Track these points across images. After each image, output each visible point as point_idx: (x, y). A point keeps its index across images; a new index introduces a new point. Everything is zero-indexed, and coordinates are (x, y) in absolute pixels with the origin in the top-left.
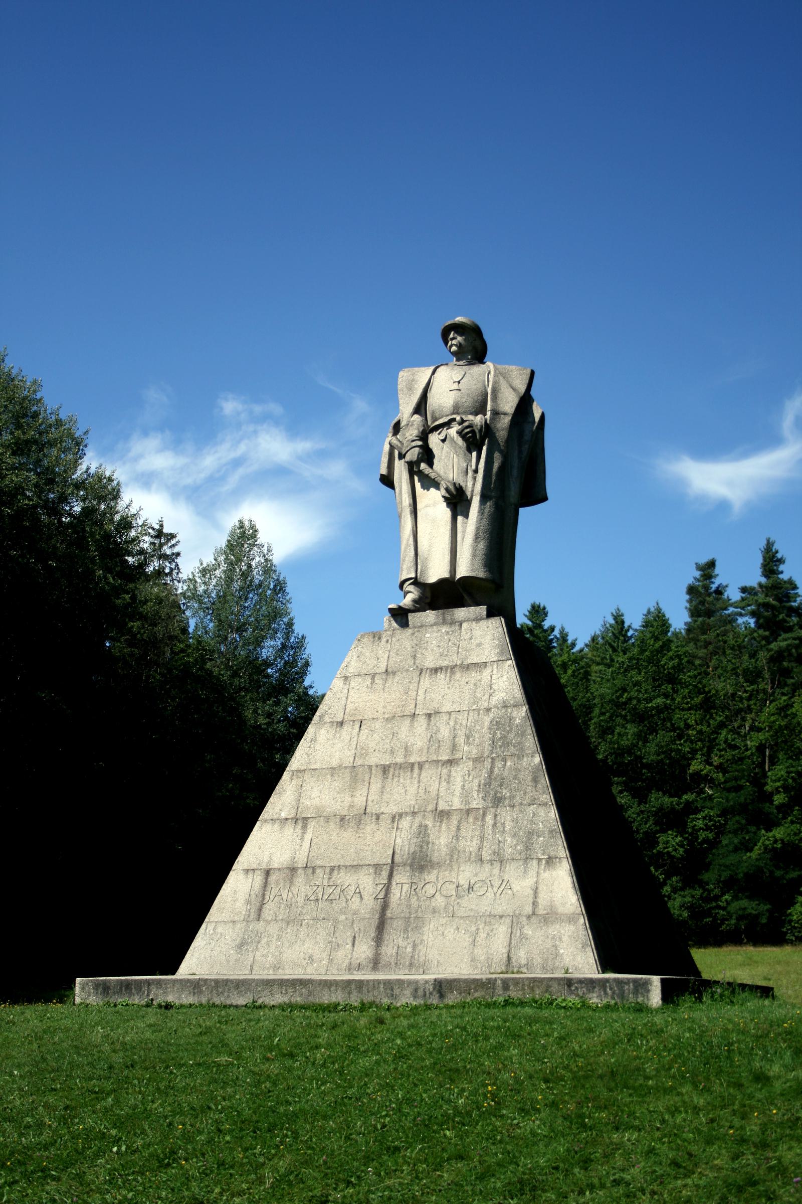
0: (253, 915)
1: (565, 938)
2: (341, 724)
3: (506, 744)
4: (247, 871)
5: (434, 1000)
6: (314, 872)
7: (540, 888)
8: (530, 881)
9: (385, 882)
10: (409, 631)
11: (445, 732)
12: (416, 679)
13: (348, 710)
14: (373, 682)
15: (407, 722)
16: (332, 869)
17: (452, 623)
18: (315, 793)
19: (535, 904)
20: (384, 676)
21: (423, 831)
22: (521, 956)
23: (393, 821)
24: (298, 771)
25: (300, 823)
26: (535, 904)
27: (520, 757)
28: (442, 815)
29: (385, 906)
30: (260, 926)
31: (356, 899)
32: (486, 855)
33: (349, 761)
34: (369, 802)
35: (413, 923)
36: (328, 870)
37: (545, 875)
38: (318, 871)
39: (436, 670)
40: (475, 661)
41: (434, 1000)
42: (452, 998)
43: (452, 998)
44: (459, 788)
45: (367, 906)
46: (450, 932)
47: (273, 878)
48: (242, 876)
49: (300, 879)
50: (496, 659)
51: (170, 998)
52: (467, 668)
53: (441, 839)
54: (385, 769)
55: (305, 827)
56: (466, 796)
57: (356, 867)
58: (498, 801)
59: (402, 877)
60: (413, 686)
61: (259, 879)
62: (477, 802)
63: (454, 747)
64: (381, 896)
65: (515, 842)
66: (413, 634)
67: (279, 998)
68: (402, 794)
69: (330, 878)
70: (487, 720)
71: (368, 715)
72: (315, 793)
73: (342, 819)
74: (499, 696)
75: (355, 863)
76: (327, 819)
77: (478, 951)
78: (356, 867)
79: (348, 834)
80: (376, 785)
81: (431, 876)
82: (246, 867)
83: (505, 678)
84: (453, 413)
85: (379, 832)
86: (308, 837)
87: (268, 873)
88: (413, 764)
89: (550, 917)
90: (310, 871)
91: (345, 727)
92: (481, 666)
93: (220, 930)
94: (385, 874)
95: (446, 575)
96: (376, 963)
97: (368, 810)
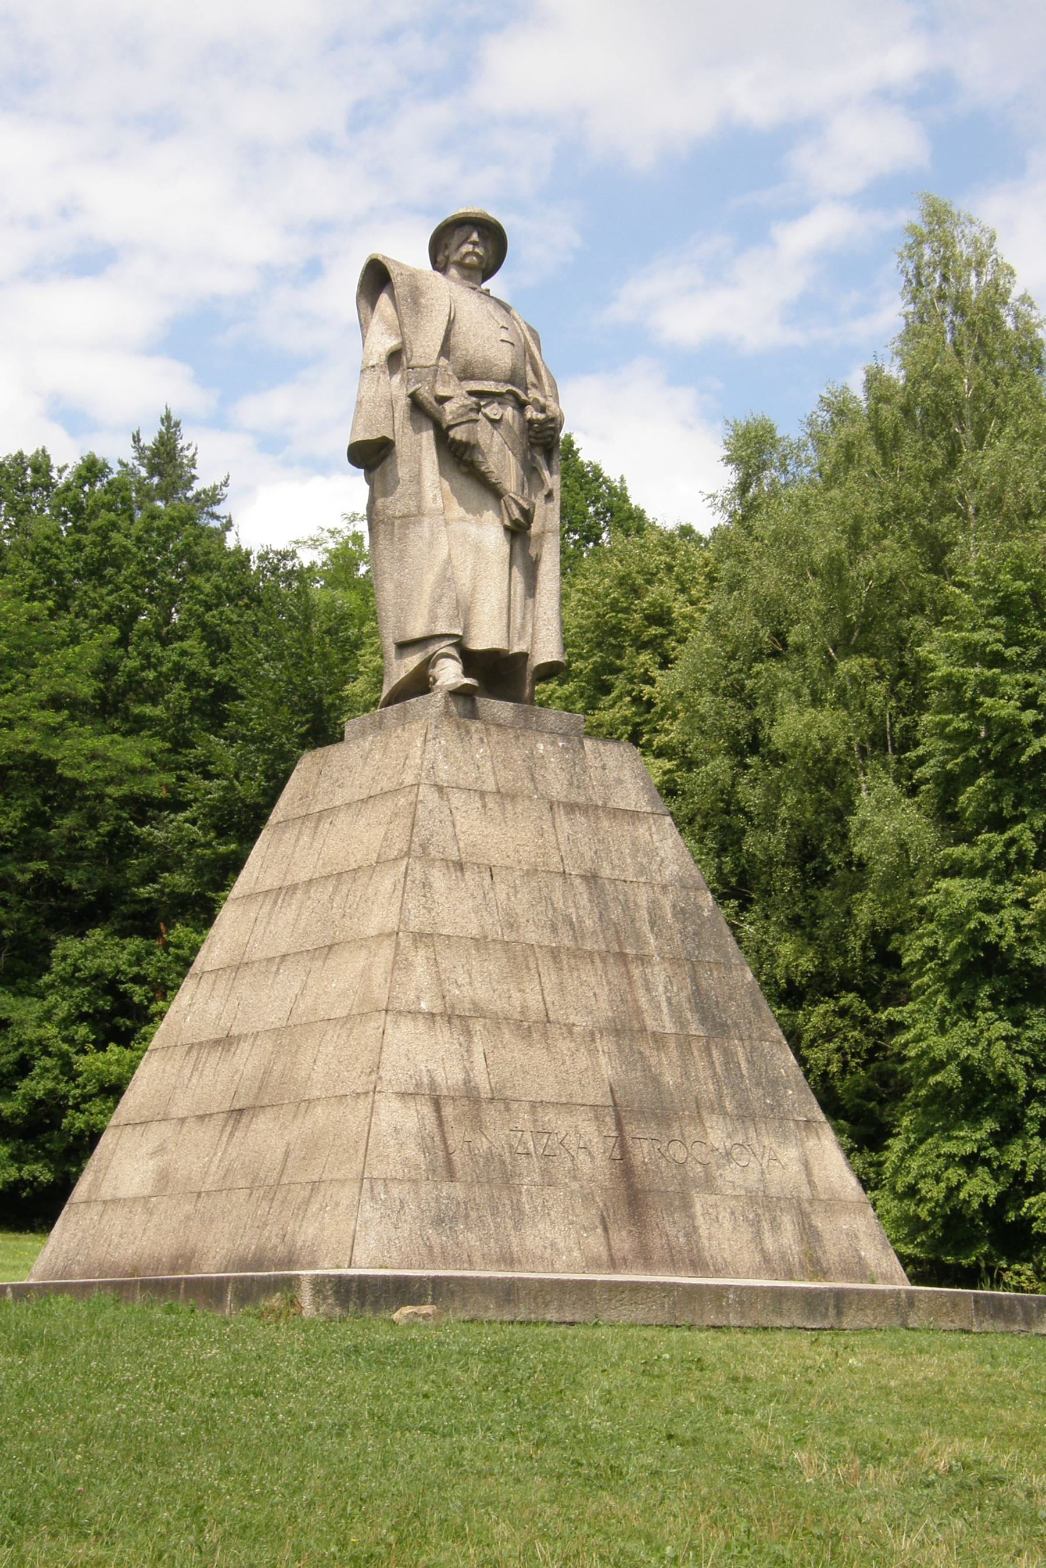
0: (441, 1171)
1: (861, 1236)
2: (460, 866)
4: (403, 1095)
6: (507, 1109)
7: (811, 1161)
9: (614, 1134)
10: (475, 726)
12: (547, 816)
13: (462, 844)
14: (484, 806)
15: (558, 882)
16: (533, 1105)
19: (811, 1183)
20: (498, 798)
23: (593, 1040)
24: (421, 935)
25: (456, 1022)
26: (811, 1183)
27: (729, 967)
31: (582, 1156)
33: (495, 931)
34: (549, 1005)
36: (527, 1107)
37: (811, 1143)
38: (514, 1106)
40: (622, 806)
48: (396, 1104)
49: (491, 1114)
50: (649, 809)
52: (616, 813)
55: (468, 1033)
60: (547, 826)
61: (427, 1110)
62: (695, 1029)
64: (617, 1154)
65: (761, 1092)
66: (517, 738)
69: (535, 1121)
70: (666, 903)
71: (496, 859)
73: (519, 1024)
74: (671, 870)
75: (564, 1100)
79: (538, 1054)
80: (550, 979)
82: (396, 1089)
83: (670, 841)
84: (507, 382)
85: (580, 1055)
86: (478, 1049)
88: (591, 954)
89: (833, 1204)
90: (501, 1106)
92: (634, 816)
94: (610, 1120)
97: (552, 1018)
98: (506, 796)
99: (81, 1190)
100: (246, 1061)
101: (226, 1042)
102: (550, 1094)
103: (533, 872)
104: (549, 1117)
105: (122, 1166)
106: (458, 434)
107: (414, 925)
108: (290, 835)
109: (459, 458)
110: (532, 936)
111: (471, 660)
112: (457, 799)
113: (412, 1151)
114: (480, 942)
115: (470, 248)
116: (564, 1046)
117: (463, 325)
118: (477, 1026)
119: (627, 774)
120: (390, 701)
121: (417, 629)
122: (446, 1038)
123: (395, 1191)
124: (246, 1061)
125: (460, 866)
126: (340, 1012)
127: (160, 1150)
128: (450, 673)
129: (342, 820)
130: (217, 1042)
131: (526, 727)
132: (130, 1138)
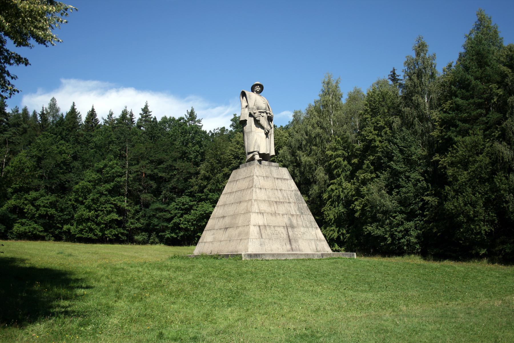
2: (261, 189)
3: (299, 200)
5: (321, 258)
8: (314, 232)
11: (285, 195)
17: (272, 166)
18: (262, 206)
21: (290, 219)
22: (319, 249)
28: (292, 215)
29: (289, 236)
30: (263, 240)
32: (304, 226)
33: (267, 199)
35: (296, 241)
39: (278, 179)
41: (321, 258)
42: (325, 257)
43: (325, 257)
44: (293, 209)
45: (285, 236)
46: (304, 243)
47: (261, 228)
49: (268, 228)
51: (267, 258)
52: (284, 179)
53: (294, 221)
54: (276, 202)
55: (263, 215)
56: (295, 211)
57: (279, 226)
58: (302, 213)
59: (290, 230)
61: (258, 228)
62: (298, 213)
63: (289, 199)
67: (292, 258)
68: (282, 209)
70: (293, 193)
71: (266, 187)
72: (262, 206)
76: (268, 213)
77: (311, 247)
78: (279, 226)
79: (274, 218)
80: (275, 206)
81: (296, 230)
86: (265, 218)
87: (259, 226)
89: (320, 240)
91: (262, 190)
92: (287, 179)
93: (254, 240)
95: (265, 152)
96: (292, 249)
98: (267, 177)
99: (200, 240)
100: (227, 220)
101: (224, 217)
102: (277, 225)
103: (272, 189)
104: (276, 228)
105: (207, 236)
106: (257, 119)
107: (254, 198)
108: (232, 184)
109: (257, 123)
110: (272, 199)
111: (261, 155)
112: (260, 178)
113: (256, 234)
114: (264, 201)
115: (258, 89)
116: (278, 217)
117: (257, 101)
118: (265, 214)
119: (286, 173)
120: (247, 162)
121: (252, 150)
122: (260, 216)
123: (254, 240)
124: (227, 220)
125: (261, 189)
126: (243, 212)
127: (214, 234)
128: (257, 157)
129: (241, 181)
130: (222, 217)
131: (270, 165)
132: (208, 232)
